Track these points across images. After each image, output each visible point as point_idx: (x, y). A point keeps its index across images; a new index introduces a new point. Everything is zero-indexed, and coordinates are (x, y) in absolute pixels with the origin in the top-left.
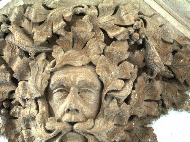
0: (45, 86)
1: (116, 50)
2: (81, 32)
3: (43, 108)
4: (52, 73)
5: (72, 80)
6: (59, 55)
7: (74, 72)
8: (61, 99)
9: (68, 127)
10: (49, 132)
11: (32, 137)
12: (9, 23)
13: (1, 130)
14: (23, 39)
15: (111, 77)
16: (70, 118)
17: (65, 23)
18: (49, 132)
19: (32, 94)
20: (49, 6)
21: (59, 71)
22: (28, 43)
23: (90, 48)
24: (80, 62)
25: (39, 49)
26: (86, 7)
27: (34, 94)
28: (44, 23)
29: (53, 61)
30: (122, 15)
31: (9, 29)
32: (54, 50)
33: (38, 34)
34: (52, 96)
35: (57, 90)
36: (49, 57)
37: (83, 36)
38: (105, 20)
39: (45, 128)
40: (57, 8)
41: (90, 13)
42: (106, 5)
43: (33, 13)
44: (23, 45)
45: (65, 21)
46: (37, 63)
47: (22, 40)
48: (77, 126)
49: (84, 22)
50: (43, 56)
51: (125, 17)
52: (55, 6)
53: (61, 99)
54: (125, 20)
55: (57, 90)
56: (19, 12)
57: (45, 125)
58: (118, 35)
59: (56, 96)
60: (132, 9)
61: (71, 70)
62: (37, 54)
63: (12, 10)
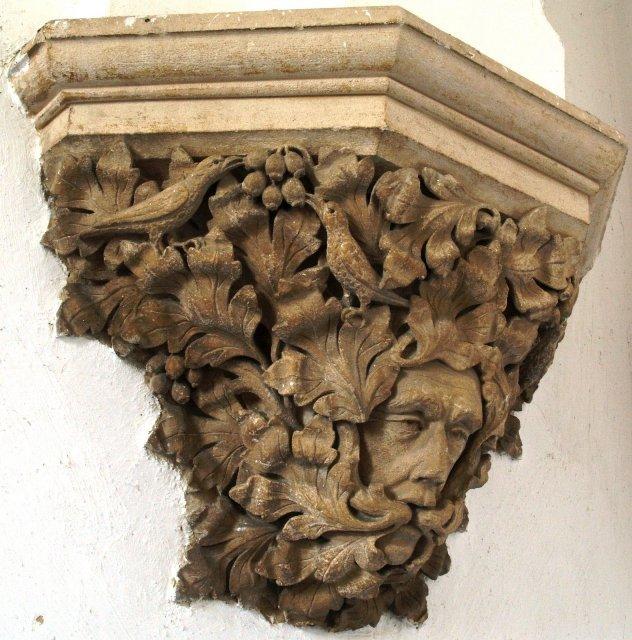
0: (378, 401)
1: (519, 342)
2: (478, 281)
3: (350, 452)
4: (402, 372)
5: (446, 404)
6: (426, 328)
7: (447, 383)
8: (403, 441)
9: (406, 512)
10: (354, 511)
11: (279, 500)
12: (309, 182)
13: (168, 445)
14: (358, 259)
15: (503, 409)
16: (422, 498)
17: (457, 250)
18: (354, 511)
19: (338, 408)
20: (435, 188)
21: (420, 372)
22: (366, 274)
23: (480, 324)
24: (464, 359)
25: (382, 297)
26: (497, 218)
27: (342, 410)
28: (407, 228)
29: (406, 340)
30: (552, 260)
31: (309, 202)
32: (414, 310)
33: (398, 260)
34: (382, 426)
35: (403, 417)
36: (398, 328)
37: (476, 291)
38: (525, 262)
39: (348, 503)
40: (448, 200)
41: (505, 236)
42: (533, 226)
43: (398, 197)
44: (353, 274)
45: (457, 243)
46: (368, 329)
47: (354, 262)
48: (429, 518)
49: (488, 257)
50: (384, 319)
51: (555, 269)
52: (446, 194)
53: (403, 441)
54: (554, 274)
55: (403, 417)
56: (361, 176)
57: (352, 494)
58: (536, 310)
59: (393, 430)
60: (572, 252)
61: (444, 376)
62: (374, 304)
63: (336, 154)
